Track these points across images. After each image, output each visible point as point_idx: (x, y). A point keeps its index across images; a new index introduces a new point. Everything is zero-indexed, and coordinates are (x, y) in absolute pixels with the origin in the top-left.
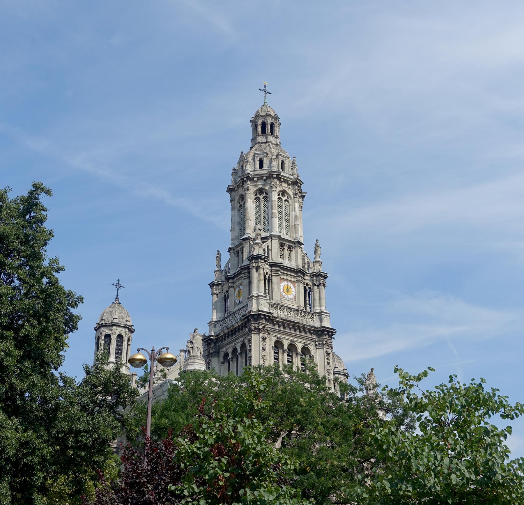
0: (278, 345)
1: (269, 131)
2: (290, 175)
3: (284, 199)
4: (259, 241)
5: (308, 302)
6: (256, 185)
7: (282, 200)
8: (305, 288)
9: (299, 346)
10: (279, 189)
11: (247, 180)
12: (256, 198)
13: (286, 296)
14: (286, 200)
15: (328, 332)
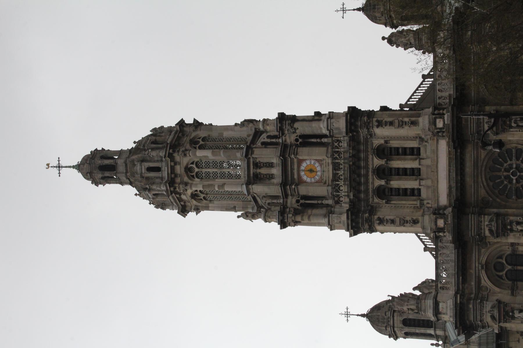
0: (383, 193)
3: (197, 170)
5: (318, 140)
7: (197, 173)
9: (377, 162)
10: (186, 179)
13: (319, 173)
14: (197, 166)
15: (351, 124)
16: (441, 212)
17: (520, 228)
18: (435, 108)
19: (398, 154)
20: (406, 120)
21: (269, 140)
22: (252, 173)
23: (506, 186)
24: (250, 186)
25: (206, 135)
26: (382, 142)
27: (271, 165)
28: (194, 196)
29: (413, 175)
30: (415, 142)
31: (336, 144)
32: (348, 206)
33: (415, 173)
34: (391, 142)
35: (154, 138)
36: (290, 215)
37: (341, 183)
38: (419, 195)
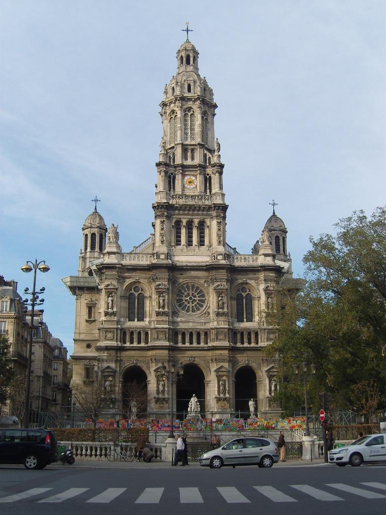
3: (189, 114)
5: (208, 187)
9: (196, 221)
13: (189, 187)
14: (191, 115)
16: (169, 257)
17: (161, 301)
18: (228, 255)
19: (200, 233)
20: (222, 238)
21: (207, 158)
22: (189, 147)
23: (184, 294)
24: (180, 146)
25: (209, 121)
27: (193, 159)
28: (173, 112)
29: (189, 242)
30: (208, 243)
31: (207, 197)
32: (171, 203)
33: (189, 243)
34: (208, 229)
35: (207, 89)
36: (165, 169)
37: (184, 200)
38: (177, 245)
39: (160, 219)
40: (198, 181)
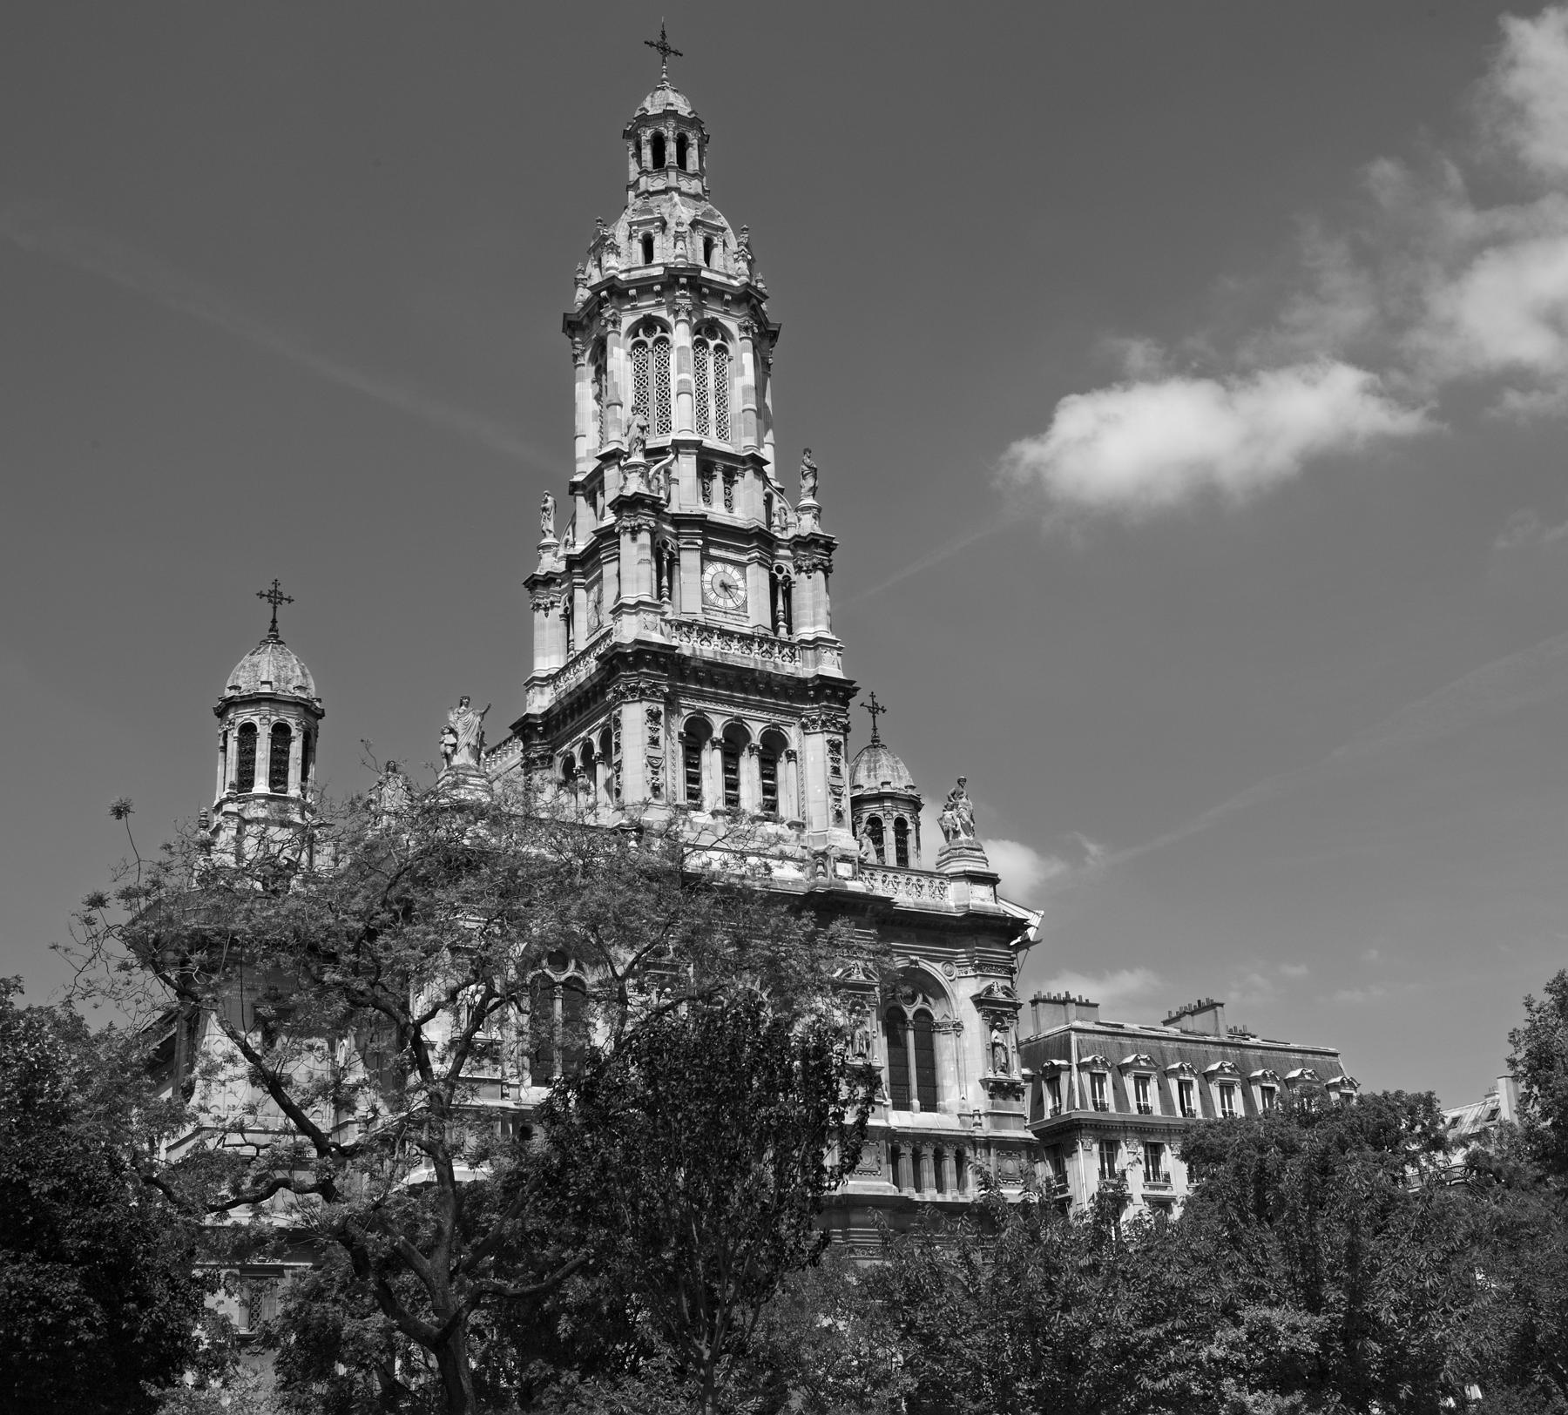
1: (674, 159)
2: (729, 277)
4: (638, 458)
6: (634, 308)
7: (707, 346)
8: (773, 578)
9: (756, 730)
11: (610, 294)
12: (634, 346)
13: (721, 602)
14: (719, 348)
26: (793, 746)
27: (729, 504)
36: (652, 524)
39: (646, 705)
40: (754, 585)
